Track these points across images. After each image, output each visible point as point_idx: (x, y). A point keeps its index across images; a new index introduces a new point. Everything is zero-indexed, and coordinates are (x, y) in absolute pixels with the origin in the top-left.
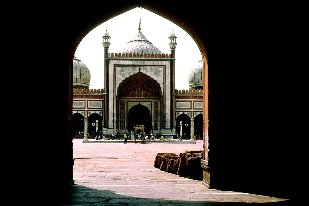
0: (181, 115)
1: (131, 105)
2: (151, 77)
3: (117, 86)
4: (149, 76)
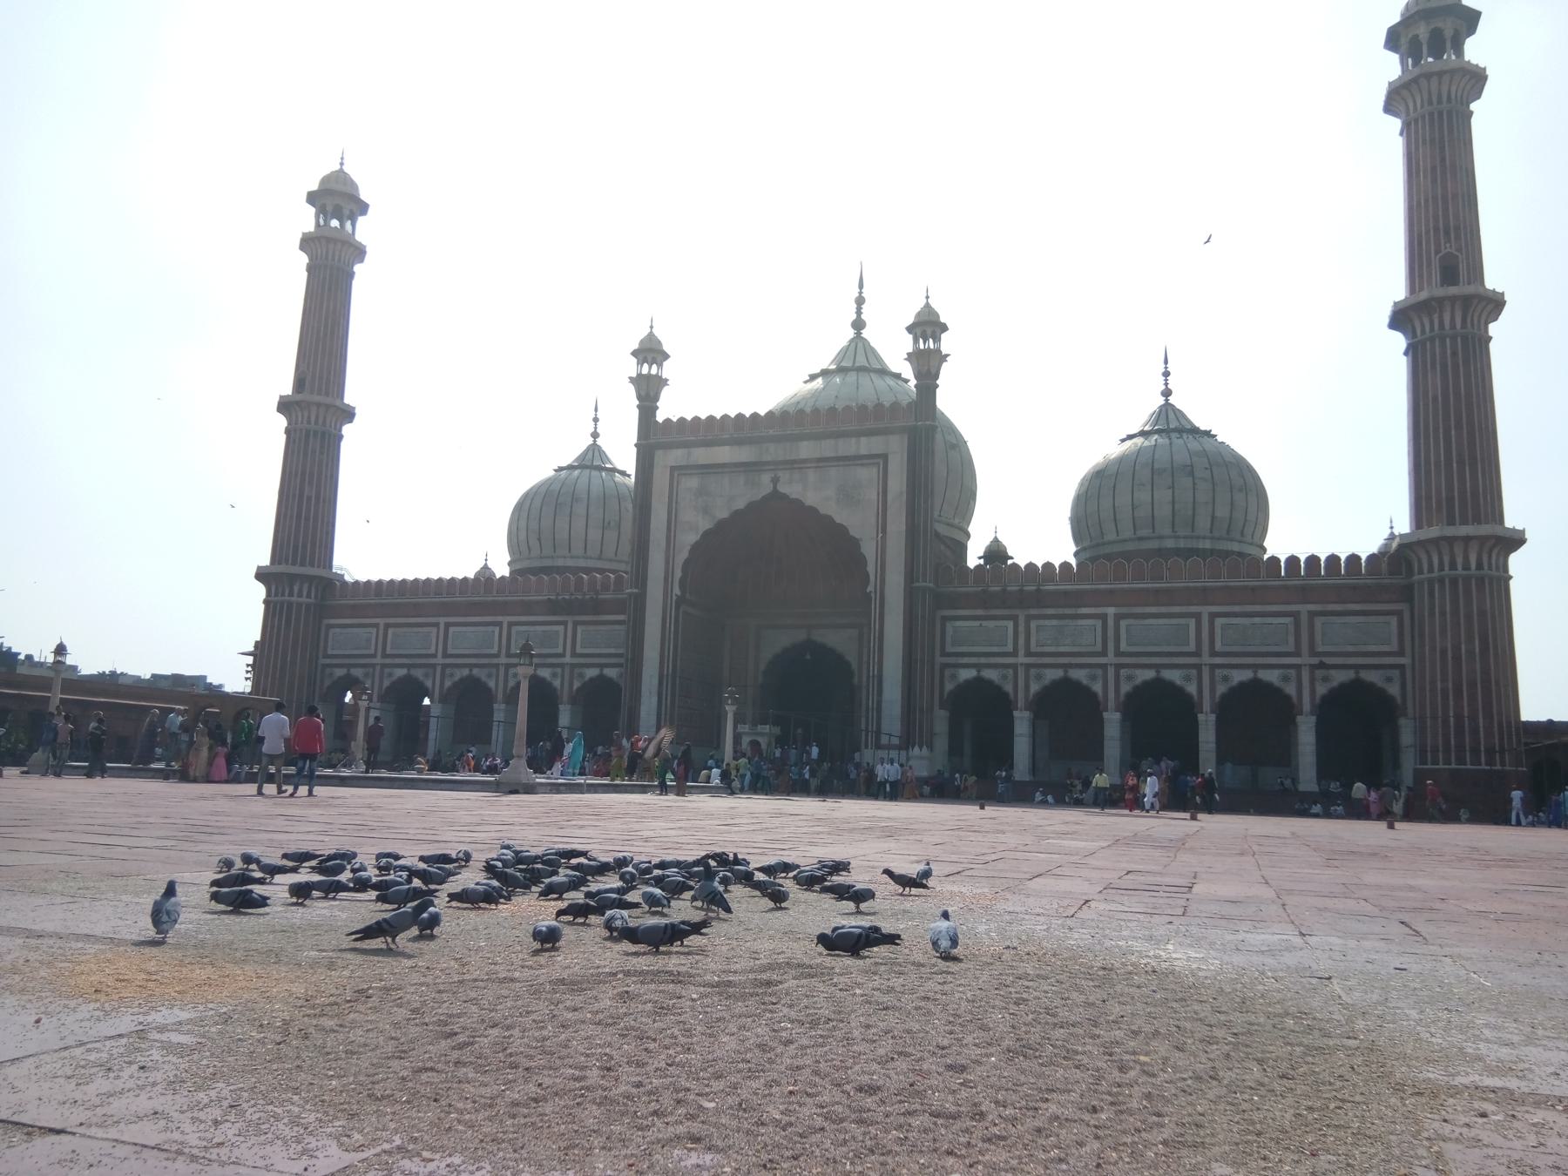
0: (968, 683)
1: (779, 641)
2: (823, 511)
3: (682, 556)
4: (813, 510)
